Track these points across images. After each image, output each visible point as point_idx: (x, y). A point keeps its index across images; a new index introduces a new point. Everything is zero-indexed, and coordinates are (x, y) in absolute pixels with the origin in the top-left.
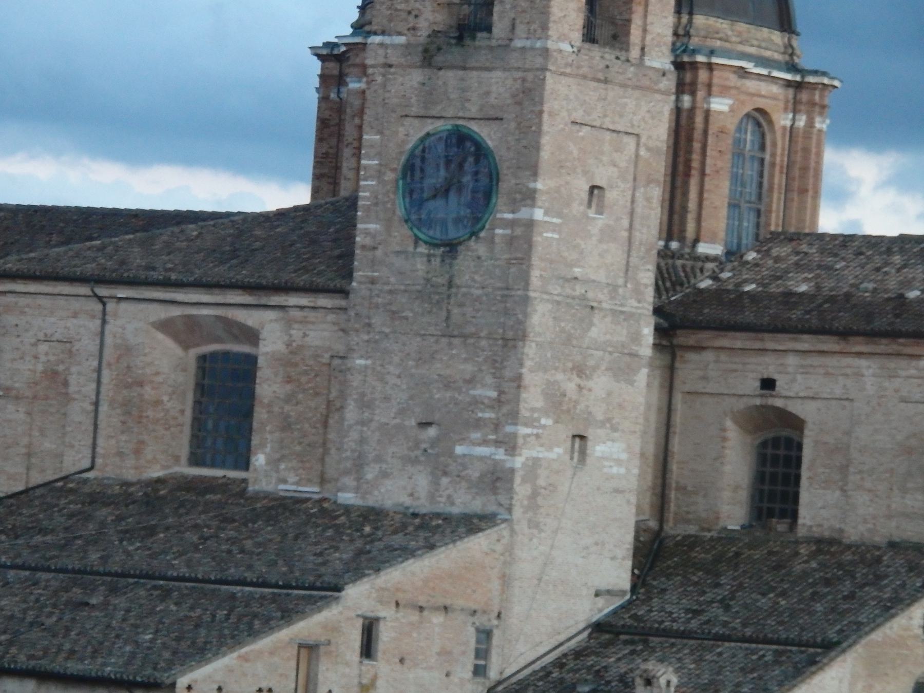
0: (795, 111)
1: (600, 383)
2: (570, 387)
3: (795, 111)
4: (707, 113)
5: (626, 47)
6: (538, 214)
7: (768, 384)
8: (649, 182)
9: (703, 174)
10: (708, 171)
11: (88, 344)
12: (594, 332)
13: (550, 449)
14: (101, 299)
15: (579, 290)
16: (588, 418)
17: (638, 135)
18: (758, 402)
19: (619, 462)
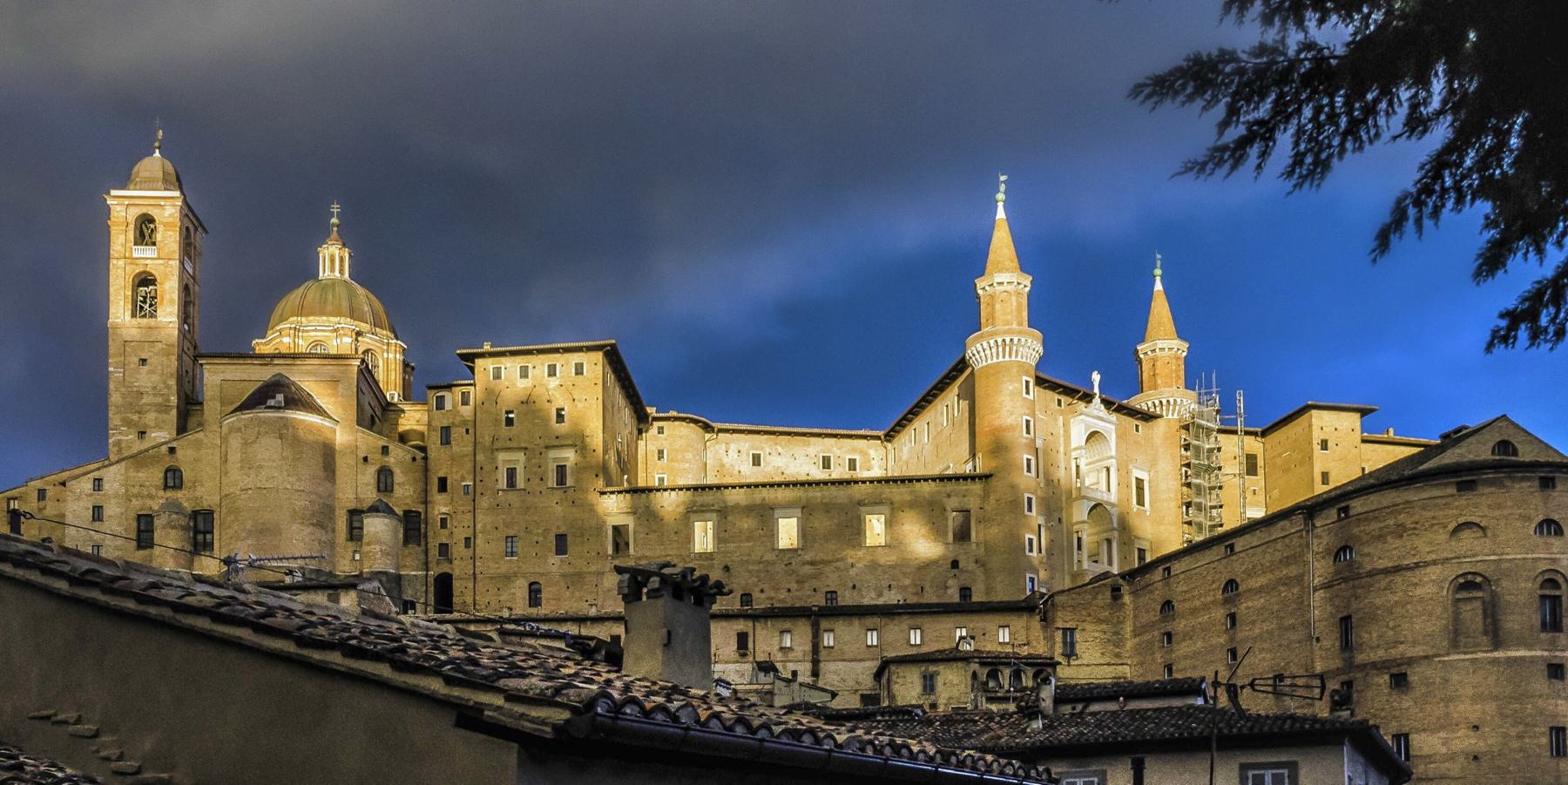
1: (150, 417)
2: (135, 417)
12: (144, 401)
15: (135, 389)
16: (146, 426)
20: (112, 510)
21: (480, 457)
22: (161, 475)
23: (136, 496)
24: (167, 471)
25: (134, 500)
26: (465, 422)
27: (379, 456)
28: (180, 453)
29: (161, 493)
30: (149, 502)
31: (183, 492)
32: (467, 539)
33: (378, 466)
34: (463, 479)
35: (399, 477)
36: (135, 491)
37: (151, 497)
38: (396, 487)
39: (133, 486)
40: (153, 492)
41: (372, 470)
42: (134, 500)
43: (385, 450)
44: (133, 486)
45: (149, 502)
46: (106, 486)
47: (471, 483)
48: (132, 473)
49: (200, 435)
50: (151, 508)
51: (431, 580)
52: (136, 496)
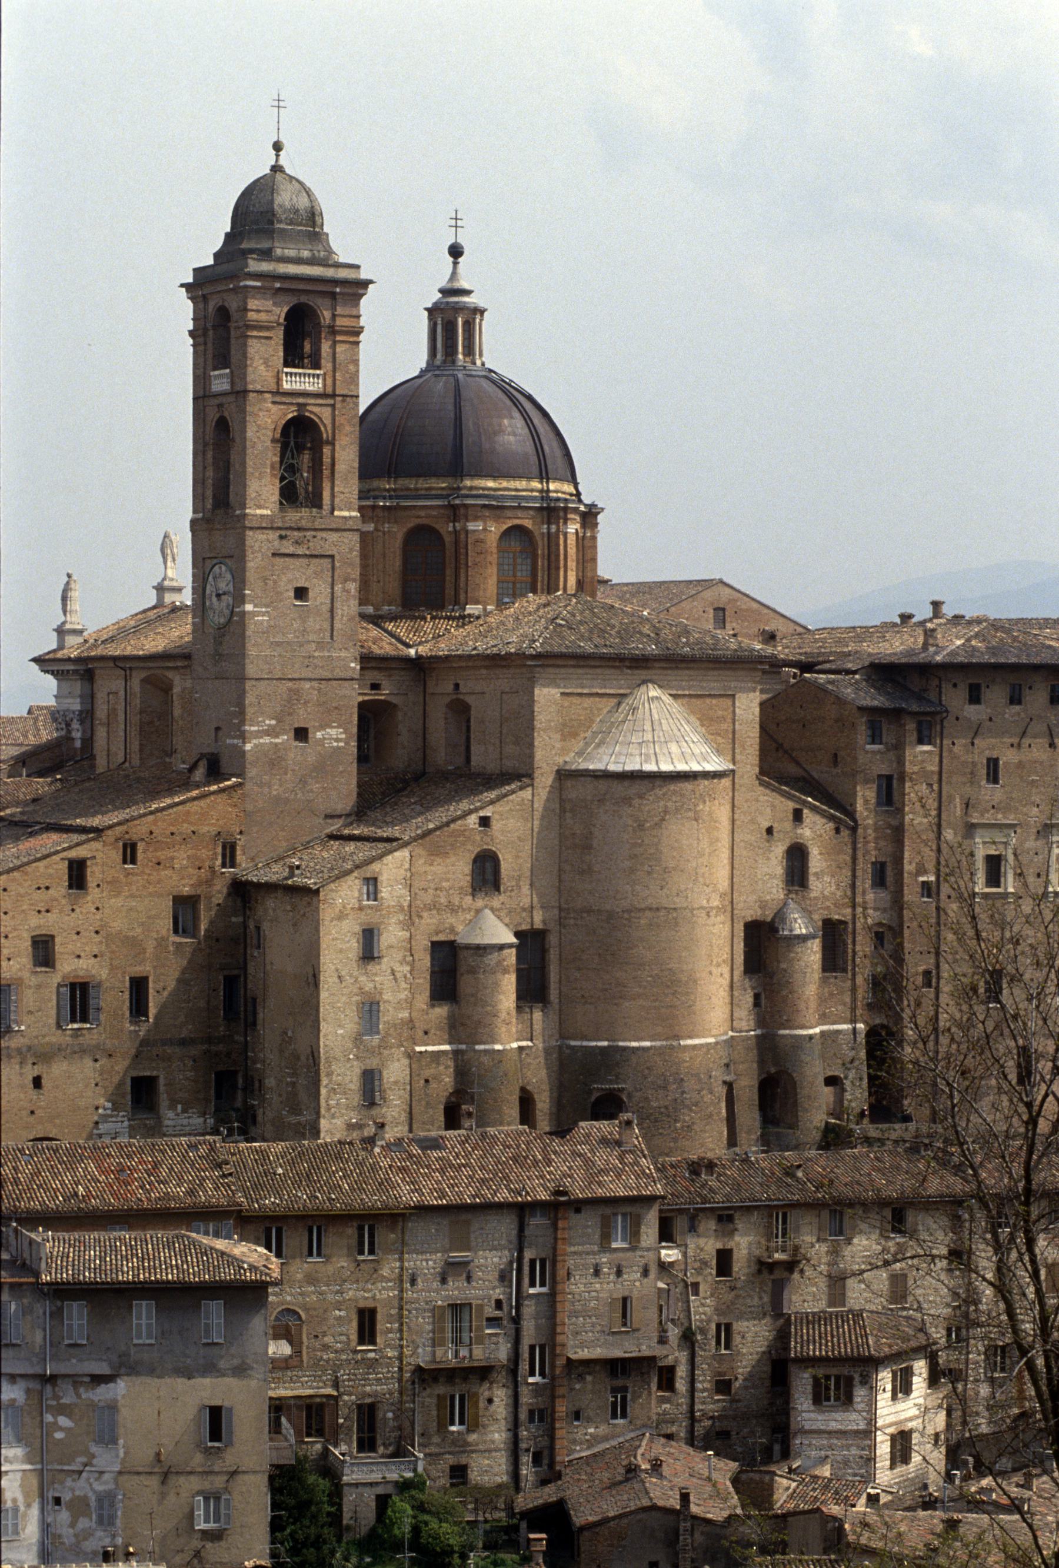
0: (549, 523)
3: (549, 523)
4: (467, 532)
5: (320, 506)
6: (249, 607)
7: (457, 686)
8: (346, 580)
9: (467, 566)
10: (470, 564)
11: (122, 693)
13: (277, 737)
14: (124, 670)
17: (332, 557)
18: (454, 697)
19: (337, 740)
20: (392, 935)
21: (948, 834)
22: (468, 869)
23: (429, 908)
24: (475, 861)
25: (425, 914)
26: (924, 773)
27: (788, 825)
28: (496, 825)
29: (468, 899)
30: (452, 920)
31: (502, 898)
32: (927, 973)
33: (785, 848)
34: (921, 870)
35: (816, 862)
36: (428, 898)
37: (453, 909)
38: (812, 881)
39: (425, 890)
40: (456, 901)
41: (779, 850)
42: (425, 914)
43: (798, 816)
44: (425, 890)
45: (452, 920)
46: (384, 892)
47: (932, 878)
48: (420, 863)
49: (527, 794)
50: (452, 930)
51: (861, 1038)
52: (429, 908)
